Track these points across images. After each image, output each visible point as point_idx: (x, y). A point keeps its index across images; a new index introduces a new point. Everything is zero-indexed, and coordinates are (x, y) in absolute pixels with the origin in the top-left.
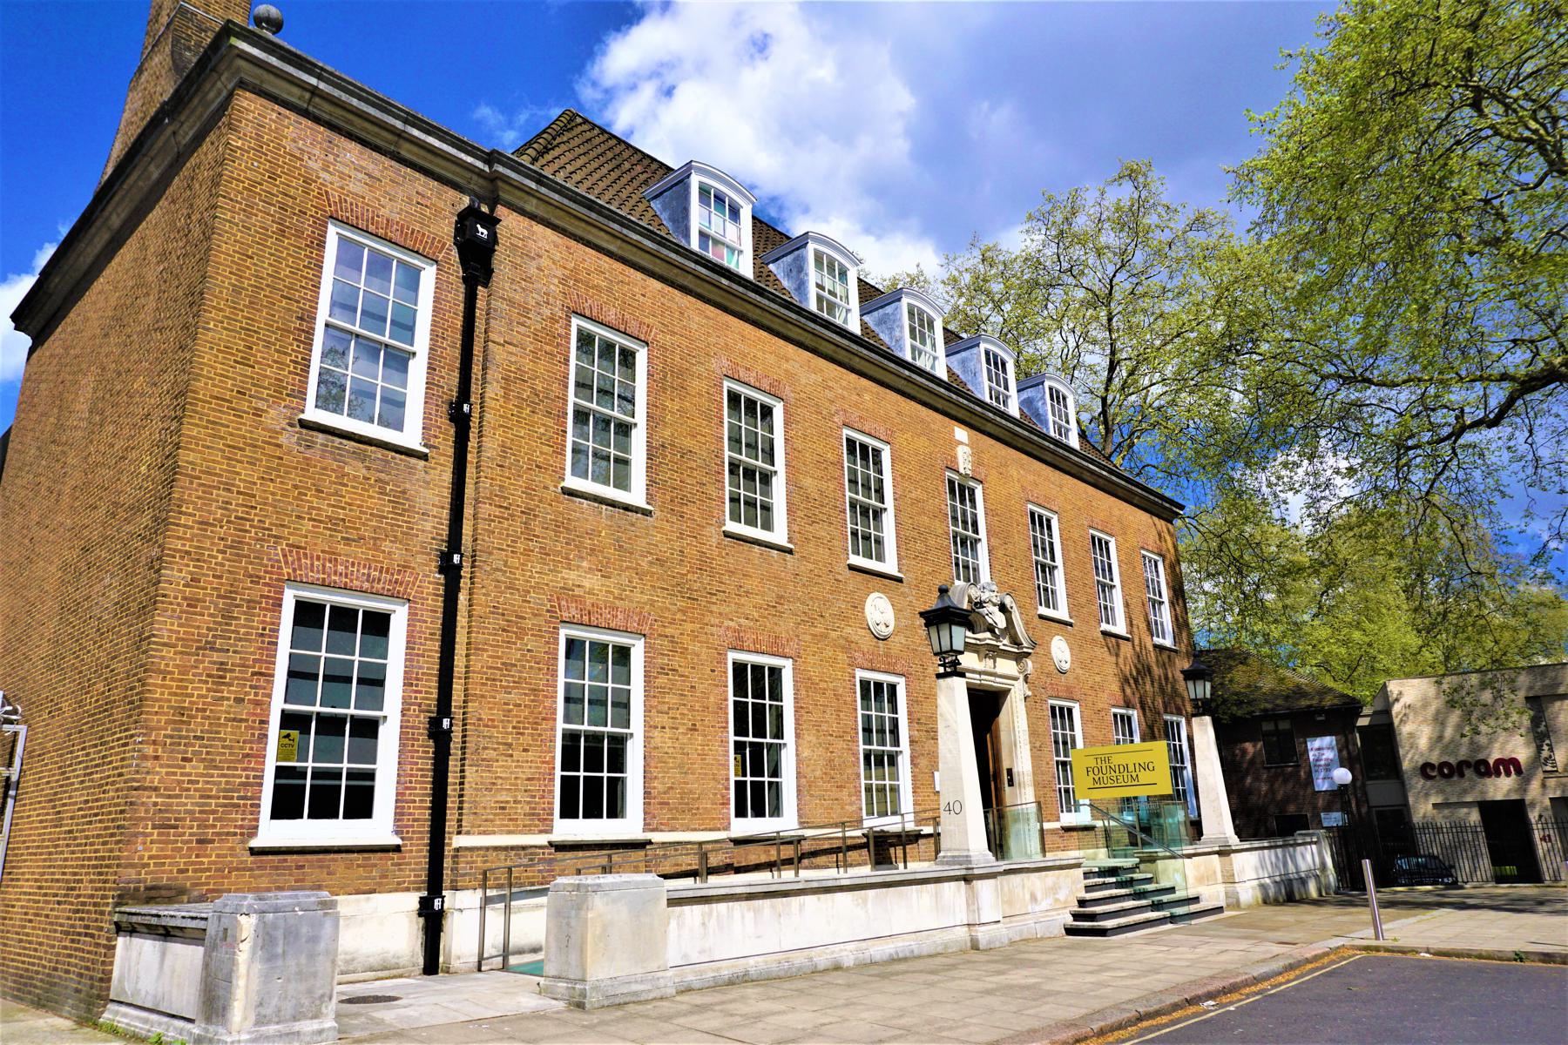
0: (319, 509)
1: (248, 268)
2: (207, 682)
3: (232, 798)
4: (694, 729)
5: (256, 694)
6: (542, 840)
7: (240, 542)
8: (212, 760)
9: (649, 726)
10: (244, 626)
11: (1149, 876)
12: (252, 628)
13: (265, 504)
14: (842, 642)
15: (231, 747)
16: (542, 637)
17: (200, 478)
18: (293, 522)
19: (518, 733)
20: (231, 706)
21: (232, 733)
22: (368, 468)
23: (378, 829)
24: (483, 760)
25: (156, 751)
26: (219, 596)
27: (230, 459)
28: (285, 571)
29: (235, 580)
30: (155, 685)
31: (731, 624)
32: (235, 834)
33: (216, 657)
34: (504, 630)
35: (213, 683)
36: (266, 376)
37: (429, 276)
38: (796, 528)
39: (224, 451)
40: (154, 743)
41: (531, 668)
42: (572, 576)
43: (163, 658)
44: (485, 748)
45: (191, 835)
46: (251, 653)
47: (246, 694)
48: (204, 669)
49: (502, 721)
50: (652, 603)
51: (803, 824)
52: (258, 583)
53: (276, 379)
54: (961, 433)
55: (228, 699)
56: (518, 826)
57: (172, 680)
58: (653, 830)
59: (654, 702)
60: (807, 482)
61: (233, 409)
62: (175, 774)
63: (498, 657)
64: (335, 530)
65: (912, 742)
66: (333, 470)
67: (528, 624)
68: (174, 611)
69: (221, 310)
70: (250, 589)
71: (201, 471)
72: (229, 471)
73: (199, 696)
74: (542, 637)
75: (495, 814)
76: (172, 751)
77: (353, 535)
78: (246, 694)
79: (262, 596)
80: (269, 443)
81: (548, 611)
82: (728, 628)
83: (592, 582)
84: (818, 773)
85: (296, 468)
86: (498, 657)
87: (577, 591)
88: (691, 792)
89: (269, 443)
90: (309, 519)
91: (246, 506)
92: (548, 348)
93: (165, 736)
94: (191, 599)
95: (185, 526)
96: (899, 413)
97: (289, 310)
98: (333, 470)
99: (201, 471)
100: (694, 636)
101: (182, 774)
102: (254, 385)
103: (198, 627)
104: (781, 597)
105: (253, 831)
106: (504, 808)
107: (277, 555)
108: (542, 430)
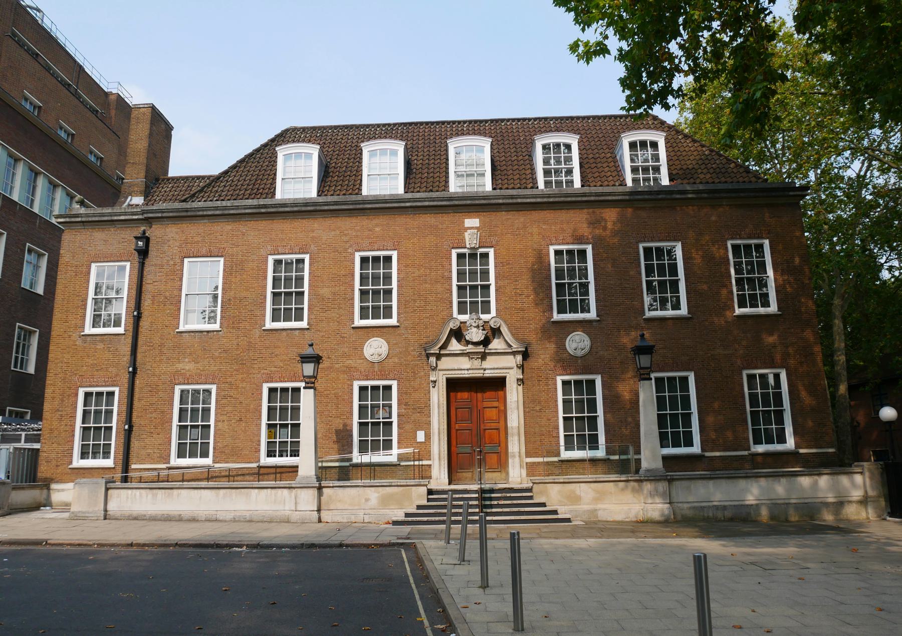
4: (241, 420)
9: (216, 421)
22: (104, 344)
33: (60, 413)
37: (128, 265)
42: (180, 366)
50: (220, 370)
59: (220, 411)
65: (399, 416)
77: (99, 368)
88: (237, 447)
100: (243, 380)
105: (71, 463)
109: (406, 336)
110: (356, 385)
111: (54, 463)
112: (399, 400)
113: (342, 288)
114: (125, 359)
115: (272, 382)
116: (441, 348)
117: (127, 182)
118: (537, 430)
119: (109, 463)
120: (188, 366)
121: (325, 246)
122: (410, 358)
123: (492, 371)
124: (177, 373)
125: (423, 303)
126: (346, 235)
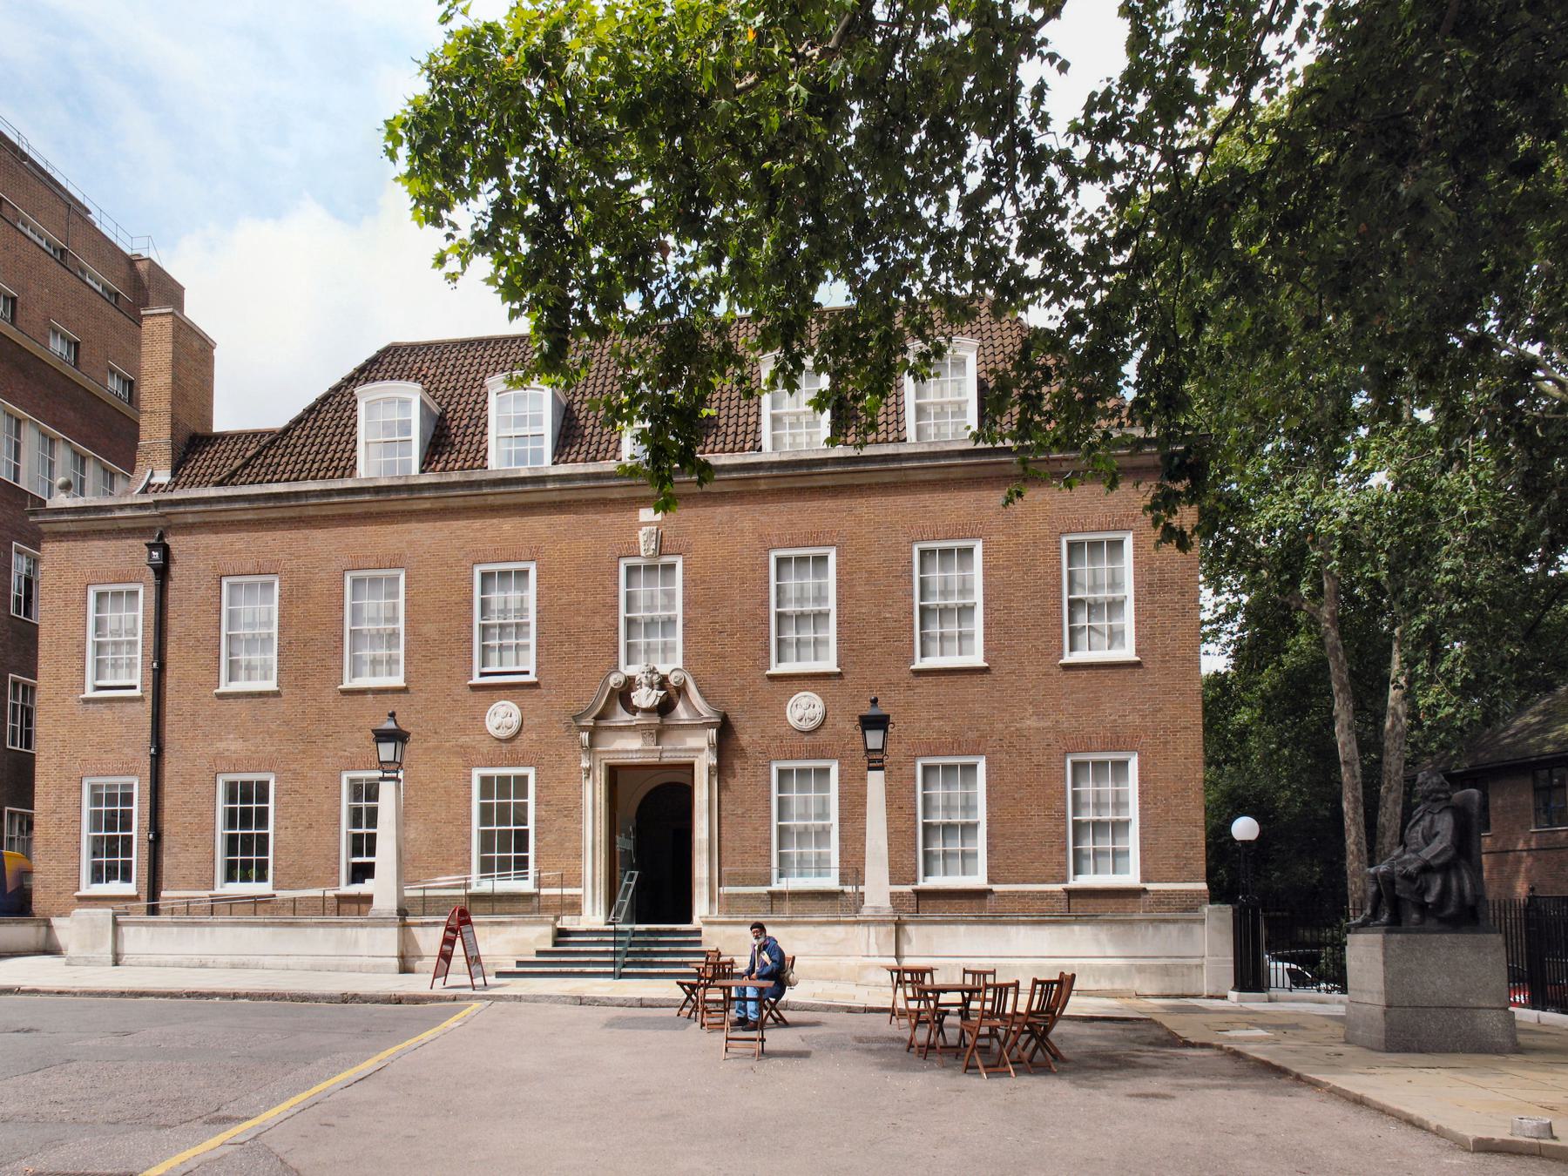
4: (310, 826)
33: (58, 816)
42: (221, 746)
67: (196, 778)
87: (226, 754)
105: (78, 889)
109: (548, 698)
110: (477, 774)
111: (54, 889)
112: (537, 798)
113: (454, 623)
115: (353, 769)
116: (597, 718)
118: (737, 844)
119: (129, 889)
120: (233, 745)
121: (428, 556)
122: (554, 733)
123: (673, 754)
124: (219, 756)
125: (573, 647)
126: (458, 537)
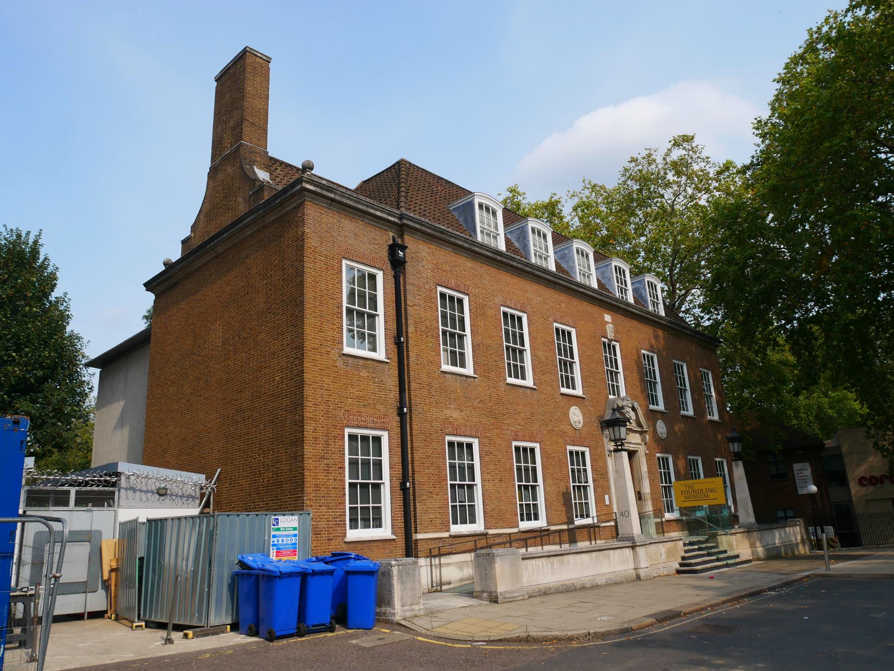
0: (353, 393)
1: (317, 287)
2: (323, 473)
3: (337, 521)
4: (501, 480)
5: (340, 476)
6: (446, 535)
7: (328, 411)
8: (329, 506)
10: (334, 448)
11: (714, 544)
12: (336, 448)
13: (335, 393)
14: (560, 433)
15: (334, 500)
16: (440, 442)
17: (312, 385)
18: (345, 400)
19: (434, 487)
20: (332, 482)
21: (334, 494)
22: (368, 372)
23: (385, 532)
24: (423, 500)
25: (310, 503)
26: (324, 436)
27: (321, 375)
28: (344, 422)
29: (328, 428)
30: (308, 475)
31: (513, 428)
32: (339, 536)
33: (326, 462)
34: (425, 441)
35: (326, 473)
36: (328, 336)
38: (536, 378)
39: (318, 372)
40: (310, 499)
41: (436, 457)
42: (448, 412)
43: (308, 464)
44: (422, 495)
45: (326, 537)
46: (337, 459)
47: (337, 477)
48: (323, 467)
49: (428, 482)
51: (549, 523)
52: (336, 428)
53: (333, 337)
54: (608, 318)
55: (331, 479)
56: (437, 529)
57: (313, 473)
58: (488, 529)
59: (484, 469)
60: (540, 354)
61: (320, 353)
62: (317, 512)
63: (424, 453)
64: (360, 402)
65: (594, 480)
66: (356, 375)
67: (434, 437)
68: (310, 443)
69: (310, 309)
70: (334, 431)
71: (312, 382)
72: (321, 381)
73: (322, 479)
74: (440, 442)
75: (429, 524)
76: (316, 503)
78: (337, 477)
79: (338, 434)
80: (333, 366)
81: (441, 430)
82: (512, 430)
83: (456, 414)
84: (554, 498)
85: (343, 376)
86: (424, 453)
87: (451, 420)
88: (502, 511)
89: (333, 366)
90: (351, 398)
91: (329, 395)
92: (429, 304)
93: (313, 496)
94: (315, 438)
95: (310, 406)
96: (578, 311)
97: (334, 304)
98: (356, 375)
99: (312, 382)
101: (320, 512)
102: (325, 340)
103: (319, 450)
104: (532, 413)
106: (431, 521)
107: (341, 415)
108: (431, 345)
111: (325, 535)
114: (392, 395)
117: (247, 146)
120: (454, 414)
124: (447, 421)
